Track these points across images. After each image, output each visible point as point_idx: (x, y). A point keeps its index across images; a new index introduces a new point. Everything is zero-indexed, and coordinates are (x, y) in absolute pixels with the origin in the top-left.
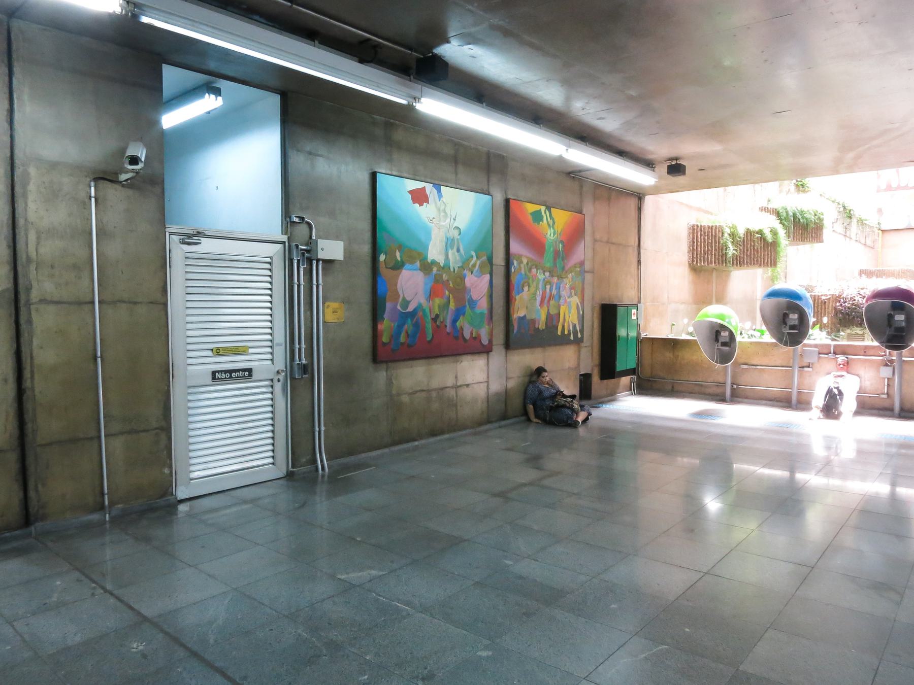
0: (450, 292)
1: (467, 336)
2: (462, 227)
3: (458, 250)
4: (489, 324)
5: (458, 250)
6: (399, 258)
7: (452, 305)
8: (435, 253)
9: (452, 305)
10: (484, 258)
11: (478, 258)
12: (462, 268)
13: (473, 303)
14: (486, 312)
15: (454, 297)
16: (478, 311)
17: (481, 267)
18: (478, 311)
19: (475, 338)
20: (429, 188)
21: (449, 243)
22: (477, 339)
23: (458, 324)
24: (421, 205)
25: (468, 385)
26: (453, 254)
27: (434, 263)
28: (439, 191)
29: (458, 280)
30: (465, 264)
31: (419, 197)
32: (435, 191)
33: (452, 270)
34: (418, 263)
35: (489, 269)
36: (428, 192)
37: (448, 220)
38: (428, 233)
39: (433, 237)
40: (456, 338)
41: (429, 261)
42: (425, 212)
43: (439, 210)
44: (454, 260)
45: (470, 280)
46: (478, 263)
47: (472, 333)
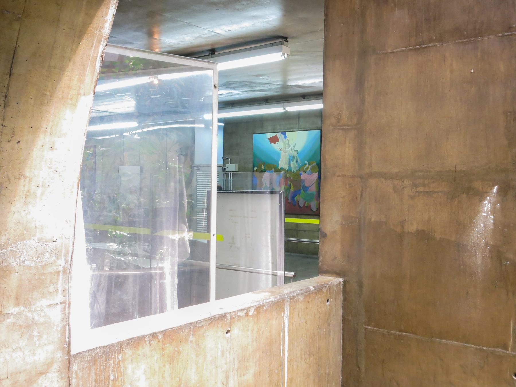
0: (291, 181)
1: (301, 205)
2: (299, 150)
3: (297, 162)
4: (317, 200)
5: (297, 162)
6: (263, 168)
7: (292, 189)
8: (283, 164)
9: (292, 189)
10: (315, 164)
11: (309, 164)
12: (299, 170)
13: (306, 188)
14: (315, 193)
15: (293, 185)
16: (309, 192)
17: (312, 169)
18: (309, 192)
19: (307, 207)
20: (279, 135)
21: (291, 159)
22: (309, 207)
23: (296, 198)
24: (275, 143)
25: (305, 231)
26: (294, 164)
27: (282, 169)
28: (285, 135)
29: (297, 176)
30: (301, 168)
31: (274, 140)
32: (283, 136)
33: (292, 171)
34: (273, 170)
35: (317, 169)
36: (278, 137)
37: (290, 148)
38: (279, 155)
39: (281, 157)
40: (295, 206)
41: (279, 168)
42: (276, 146)
43: (285, 144)
44: (294, 166)
45: (303, 176)
46: (310, 167)
47: (305, 204)
